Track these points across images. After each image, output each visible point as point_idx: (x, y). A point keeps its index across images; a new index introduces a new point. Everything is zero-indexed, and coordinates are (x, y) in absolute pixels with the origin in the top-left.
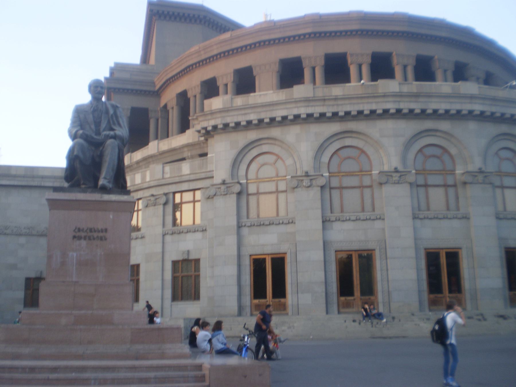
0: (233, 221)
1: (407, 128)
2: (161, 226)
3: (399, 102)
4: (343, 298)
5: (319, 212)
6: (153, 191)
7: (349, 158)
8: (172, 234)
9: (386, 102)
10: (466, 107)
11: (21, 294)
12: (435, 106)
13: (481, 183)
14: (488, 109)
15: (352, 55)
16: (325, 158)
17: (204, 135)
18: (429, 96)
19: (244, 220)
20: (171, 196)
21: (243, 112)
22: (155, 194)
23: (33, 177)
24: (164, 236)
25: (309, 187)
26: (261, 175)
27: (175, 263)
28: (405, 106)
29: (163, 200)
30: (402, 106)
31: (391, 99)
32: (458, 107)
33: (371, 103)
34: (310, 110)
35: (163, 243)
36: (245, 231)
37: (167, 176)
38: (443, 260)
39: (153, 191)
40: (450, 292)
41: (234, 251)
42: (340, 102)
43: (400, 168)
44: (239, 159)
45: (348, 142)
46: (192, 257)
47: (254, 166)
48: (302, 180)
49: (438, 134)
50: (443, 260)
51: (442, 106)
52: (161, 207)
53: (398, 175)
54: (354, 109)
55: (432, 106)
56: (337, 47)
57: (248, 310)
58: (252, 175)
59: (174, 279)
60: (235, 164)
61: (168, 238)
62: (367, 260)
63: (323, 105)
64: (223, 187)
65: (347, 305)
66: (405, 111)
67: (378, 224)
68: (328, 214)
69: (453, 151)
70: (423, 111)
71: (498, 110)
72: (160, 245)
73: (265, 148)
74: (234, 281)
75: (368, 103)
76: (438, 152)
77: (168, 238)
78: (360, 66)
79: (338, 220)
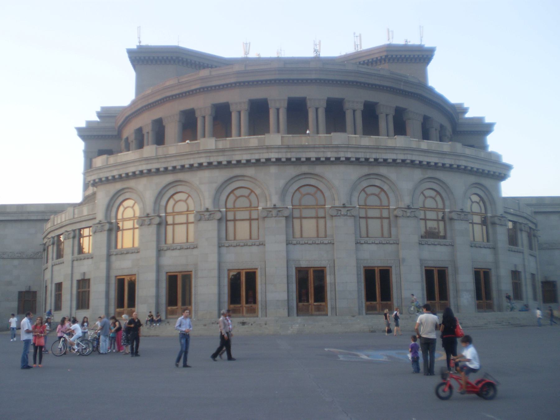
0: (104, 251)
1: (220, 176)
2: (71, 255)
3: (210, 156)
4: (169, 308)
5: (154, 244)
7: (180, 201)
8: (77, 260)
9: (200, 157)
10: (264, 156)
12: (238, 158)
13: (275, 217)
14: (283, 156)
16: (163, 203)
18: (232, 150)
19: (113, 251)
20: (77, 232)
21: (109, 169)
22: (68, 230)
23: (22, 213)
24: (73, 261)
25: (149, 225)
26: (125, 216)
27: (79, 281)
28: (214, 159)
29: (72, 235)
30: (212, 160)
31: (203, 155)
32: (257, 157)
33: (190, 159)
34: (149, 167)
35: (72, 267)
36: (113, 258)
37: (76, 216)
39: (69, 228)
40: (247, 302)
42: (168, 160)
43: (211, 208)
44: (111, 204)
45: (179, 188)
46: (86, 278)
47: (121, 209)
48: (145, 220)
49: (246, 178)
51: (244, 157)
52: (71, 240)
53: (208, 213)
54: (177, 164)
56: (221, 98)
58: (120, 216)
59: (78, 293)
61: (75, 263)
62: (187, 277)
63: (158, 163)
64: (99, 226)
65: (173, 313)
66: (215, 163)
67: (195, 252)
68: (163, 245)
69: (258, 191)
70: (229, 162)
71: (293, 156)
72: (70, 269)
74: (103, 295)
75: (187, 159)
76: (246, 192)
77: (75, 263)
79: (168, 249)
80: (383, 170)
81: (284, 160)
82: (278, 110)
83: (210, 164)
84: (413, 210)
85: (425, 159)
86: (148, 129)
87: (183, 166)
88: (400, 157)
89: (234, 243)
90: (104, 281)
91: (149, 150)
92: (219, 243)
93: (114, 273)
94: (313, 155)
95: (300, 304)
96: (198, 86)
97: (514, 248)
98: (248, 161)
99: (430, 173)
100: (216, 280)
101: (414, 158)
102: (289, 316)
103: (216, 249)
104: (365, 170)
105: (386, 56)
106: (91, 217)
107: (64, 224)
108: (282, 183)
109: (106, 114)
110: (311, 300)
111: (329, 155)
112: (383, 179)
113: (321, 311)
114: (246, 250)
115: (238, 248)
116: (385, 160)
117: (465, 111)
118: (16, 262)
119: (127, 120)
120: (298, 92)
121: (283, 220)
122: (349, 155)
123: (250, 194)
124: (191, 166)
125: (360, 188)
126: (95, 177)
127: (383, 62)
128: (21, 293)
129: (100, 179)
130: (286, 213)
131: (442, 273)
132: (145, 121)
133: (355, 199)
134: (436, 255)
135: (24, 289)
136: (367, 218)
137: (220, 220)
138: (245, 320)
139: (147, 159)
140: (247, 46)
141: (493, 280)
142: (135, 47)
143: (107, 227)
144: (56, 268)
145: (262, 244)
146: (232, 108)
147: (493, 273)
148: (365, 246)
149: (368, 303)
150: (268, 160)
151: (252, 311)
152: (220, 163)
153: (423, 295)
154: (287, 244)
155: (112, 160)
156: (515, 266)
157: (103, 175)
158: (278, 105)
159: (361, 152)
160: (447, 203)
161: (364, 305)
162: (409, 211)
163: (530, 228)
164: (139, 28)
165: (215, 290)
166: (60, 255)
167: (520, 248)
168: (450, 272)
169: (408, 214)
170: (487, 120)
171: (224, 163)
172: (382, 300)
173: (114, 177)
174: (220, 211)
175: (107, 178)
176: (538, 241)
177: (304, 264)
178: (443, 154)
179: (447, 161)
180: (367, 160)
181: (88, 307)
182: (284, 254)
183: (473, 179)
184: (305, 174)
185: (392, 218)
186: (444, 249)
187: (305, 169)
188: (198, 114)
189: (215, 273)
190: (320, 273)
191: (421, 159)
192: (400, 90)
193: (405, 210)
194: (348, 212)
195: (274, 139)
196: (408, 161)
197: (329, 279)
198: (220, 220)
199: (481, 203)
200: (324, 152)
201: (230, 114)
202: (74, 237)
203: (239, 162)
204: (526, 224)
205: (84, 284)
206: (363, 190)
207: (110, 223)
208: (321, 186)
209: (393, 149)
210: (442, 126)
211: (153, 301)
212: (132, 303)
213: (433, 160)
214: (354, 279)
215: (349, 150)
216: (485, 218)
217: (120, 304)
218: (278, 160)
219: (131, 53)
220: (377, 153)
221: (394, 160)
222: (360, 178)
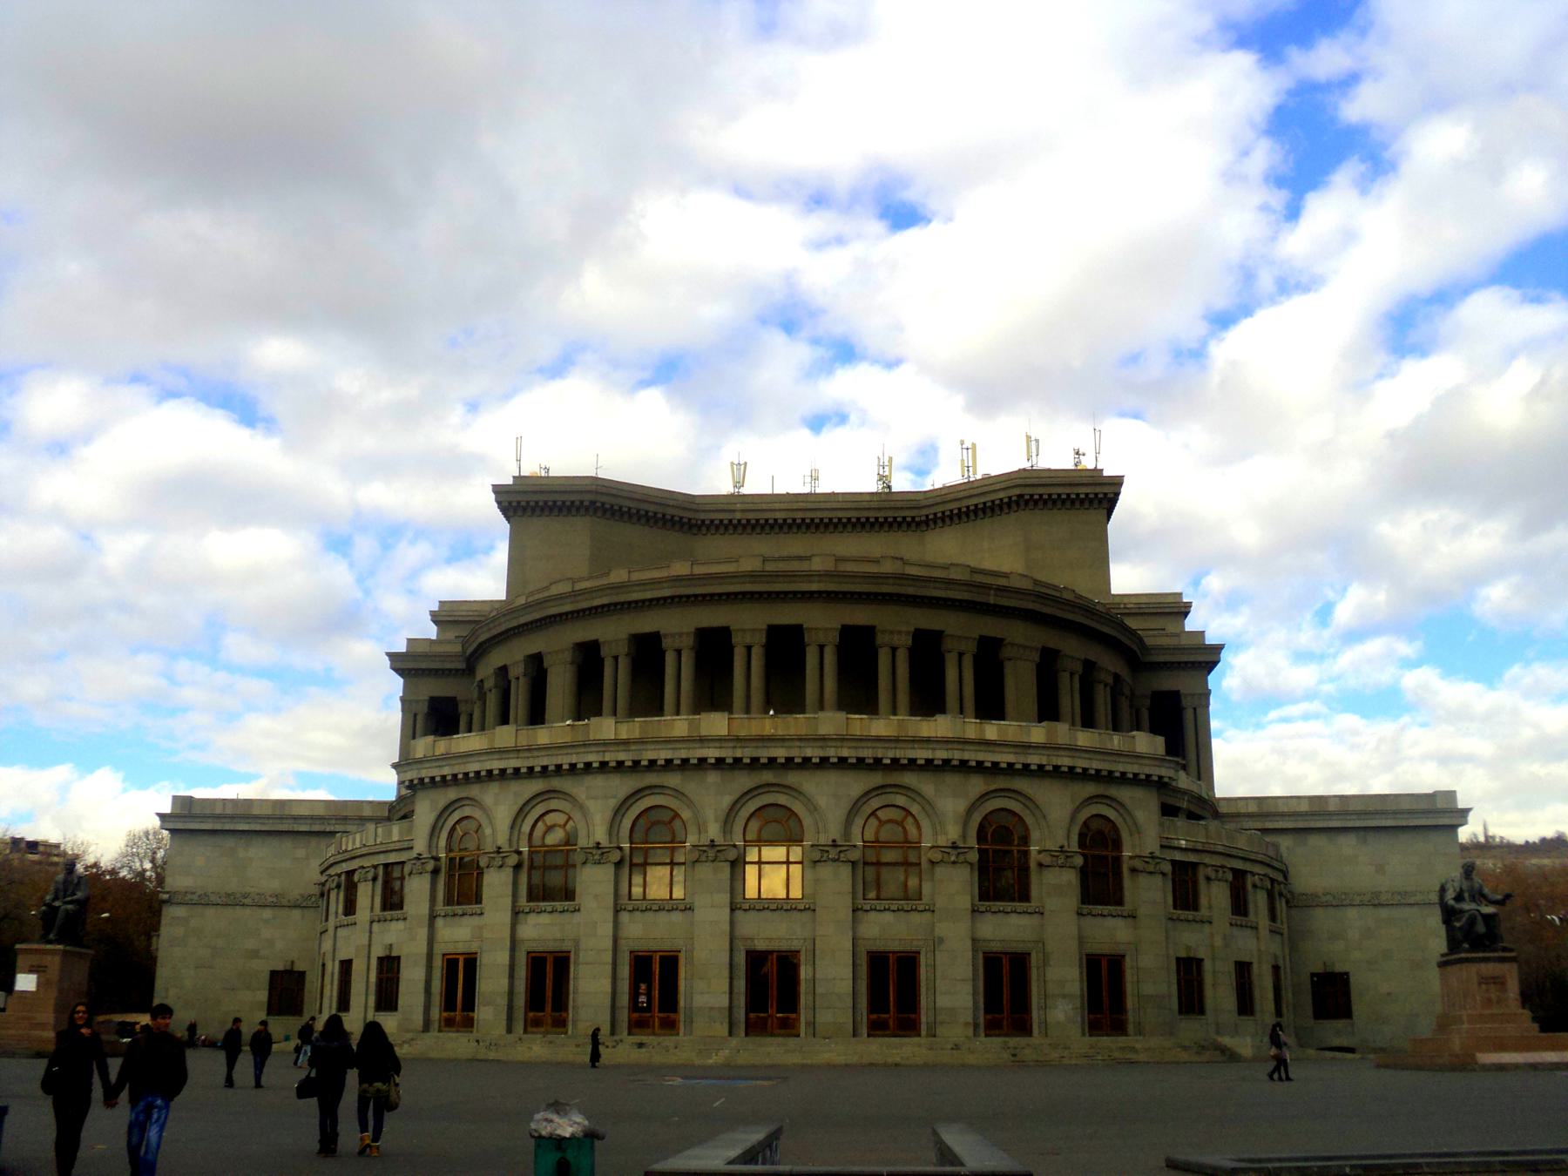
1: (621, 786)
4: (531, 1014)
5: (509, 901)
6: (367, 862)
10: (695, 753)
11: (263, 996)
12: (651, 755)
14: (728, 754)
15: (666, 636)
16: (526, 828)
17: (408, 787)
20: (381, 871)
23: (281, 818)
28: (611, 757)
29: (370, 876)
34: (502, 764)
36: (440, 922)
38: (656, 968)
39: (367, 862)
41: (424, 949)
43: (604, 842)
45: (554, 804)
50: (656, 968)
51: (662, 755)
54: (550, 762)
55: (647, 755)
56: (646, 623)
57: (436, 1025)
60: (434, 830)
61: (375, 926)
65: (537, 1023)
69: (686, 814)
70: (636, 763)
71: (746, 753)
73: (467, 811)
74: (422, 986)
77: (375, 926)
78: (679, 652)
80: (909, 779)
81: (729, 761)
82: (749, 648)
83: (604, 764)
85: (988, 757)
86: (517, 671)
87: (559, 767)
88: (940, 754)
89: (644, 905)
90: (424, 962)
91: (505, 736)
92: (616, 904)
93: (439, 949)
94: (780, 753)
95: (752, 1015)
96: (605, 601)
97: (1183, 914)
98: (669, 762)
99: (1001, 782)
100: (609, 968)
101: (966, 756)
102: (731, 1034)
103: (610, 915)
104: (877, 779)
105: (1021, 496)
106: (406, 845)
107: (358, 852)
108: (727, 801)
109: (448, 616)
111: (809, 753)
113: (788, 1027)
114: (663, 917)
115: (649, 914)
116: (912, 761)
117: (1183, 610)
118: (267, 913)
119: (483, 649)
120: (786, 615)
121: (727, 868)
122: (845, 753)
123: (673, 819)
124: (573, 766)
125: (867, 810)
126: (412, 774)
127: (1014, 507)
128: (273, 973)
129: (421, 780)
130: (732, 854)
132: (513, 655)
133: (856, 830)
134: (1007, 928)
135: (280, 967)
136: (878, 864)
137: (618, 864)
138: (644, 1039)
139: (502, 752)
140: (740, 470)
141: (1129, 976)
142: (510, 481)
143: (430, 866)
144: (342, 932)
145: (689, 909)
146: (666, 643)
147: (1128, 962)
148: (873, 915)
149: (874, 1016)
150: (702, 760)
151: (670, 1026)
152: (620, 764)
153: (975, 1003)
154: (732, 910)
155: (442, 745)
157: (426, 773)
158: (748, 640)
161: (865, 1020)
163: (1239, 875)
164: (519, 439)
165: (606, 985)
166: (350, 908)
167: (1204, 912)
170: (1210, 639)
171: (629, 763)
173: (444, 777)
174: (620, 849)
175: (433, 778)
176: (1281, 895)
177: (761, 946)
178: (1027, 747)
179: (1034, 760)
180: (878, 761)
181: (396, 1009)
182: (727, 927)
183: (1091, 789)
184: (768, 785)
185: (925, 864)
186: (1024, 921)
187: (768, 777)
188: (605, 652)
189: (608, 957)
190: (787, 963)
191: (981, 757)
192: (988, 604)
195: (716, 723)
196: (955, 763)
197: (804, 973)
198: (618, 864)
201: (662, 653)
202: (374, 879)
203: (652, 762)
204: (1222, 867)
205: (389, 967)
206: (873, 813)
207: (437, 859)
208: (797, 807)
209: (928, 741)
210: (1089, 666)
211: (503, 1002)
212: (469, 1005)
213: (1004, 758)
214: (847, 972)
216: (1118, 860)
217: (449, 1003)
218: (720, 762)
219: (499, 490)
221: (929, 762)
222: (867, 793)
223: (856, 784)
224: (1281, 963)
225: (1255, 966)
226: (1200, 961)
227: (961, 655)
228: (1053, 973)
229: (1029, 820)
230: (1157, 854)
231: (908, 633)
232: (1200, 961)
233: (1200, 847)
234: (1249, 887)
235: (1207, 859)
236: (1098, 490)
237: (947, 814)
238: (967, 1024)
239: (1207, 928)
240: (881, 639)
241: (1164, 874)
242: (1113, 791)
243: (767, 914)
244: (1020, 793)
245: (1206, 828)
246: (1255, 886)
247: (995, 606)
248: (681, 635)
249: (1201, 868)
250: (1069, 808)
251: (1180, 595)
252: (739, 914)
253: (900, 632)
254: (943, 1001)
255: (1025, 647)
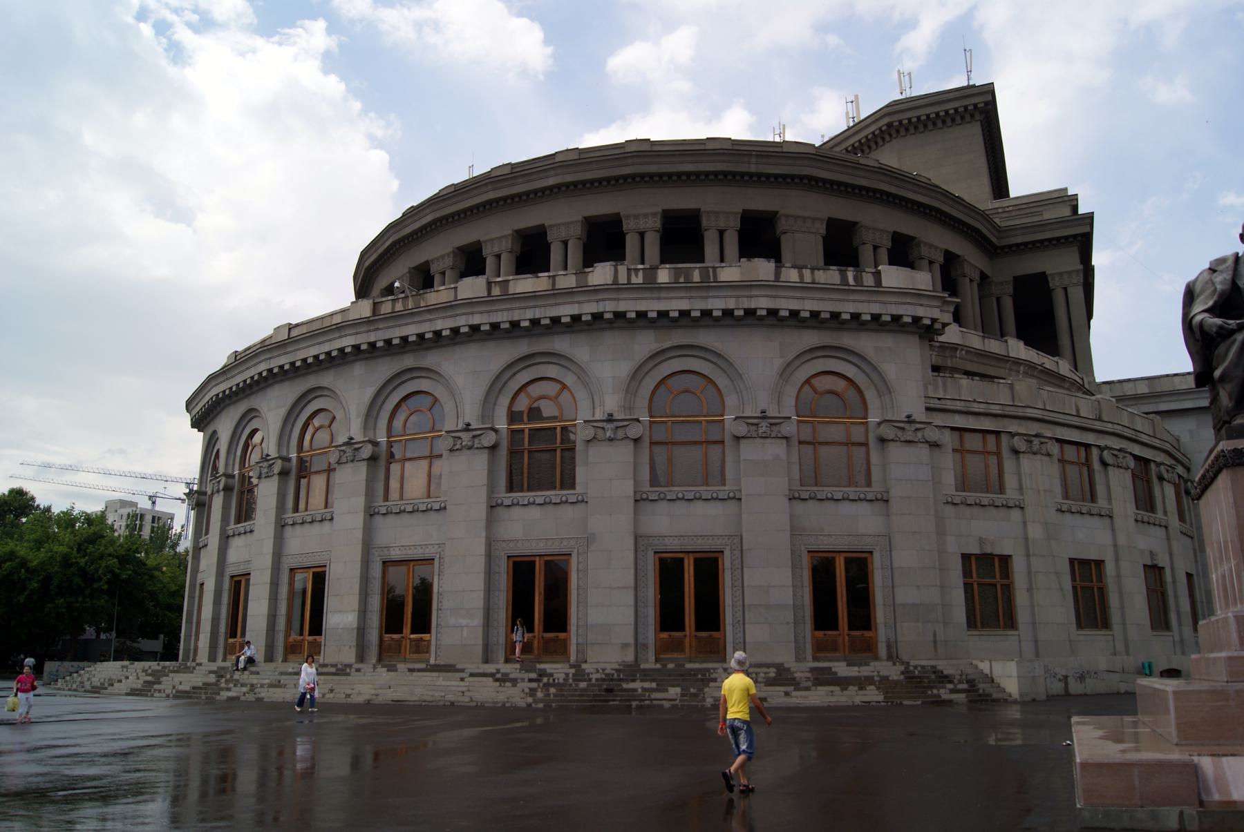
80: (561, 344)
84: (621, 424)
99: (679, 337)
105: (889, 125)
108: (369, 392)
110: (407, 629)
111: (439, 325)
112: (562, 362)
120: (530, 218)
122: (476, 320)
131: (709, 567)
141: (878, 580)
147: (877, 562)
148: (516, 511)
156: (981, 541)
158: (496, 249)
159: (502, 310)
160: (731, 400)
162: (609, 426)
168: (727, 561)
169: (608, 434)
172: (546, 630)
180: (515, 324)
183: (811, 338)
186: (714, 509)
187: (408, 361)
192: (751, 175)
193: (604, 425)
194: (476, 441)
199: (852, 392)
200: (430, 320)
214: (479, 583)
215: (476, 310)
220: (535, 307)
221: (576, 318)
222: (509, 366)
223: (496, 357)
224: (1163, 561)
225: (1110, 569)
226: (1005, 560)
227: (721, 233)
228: (753, 577)
229: (722, 382)
230: (920, 415)
231: (654, 215)
232: (1005, 560)
233: (995, 409)
234: (1096, 465)
235: (1013, 427)
236: (966, 102)
237: (603, 379)
238: (625, 646)
239: (1015, 514)
240: (627, 225)
241: (935, 445)
242: (847, 340)
243: (406, 516)
244: (706, 350)
245: (1011, 386)
246: (1105, 464)
247: (759, 175)
248: (443, 257)
249: (1004, 438)
250: (778, 363)
251: (1066, 189)
252: (379, 520)
253: (646, 215)
254: (595, 616)
255: (805, 219)
